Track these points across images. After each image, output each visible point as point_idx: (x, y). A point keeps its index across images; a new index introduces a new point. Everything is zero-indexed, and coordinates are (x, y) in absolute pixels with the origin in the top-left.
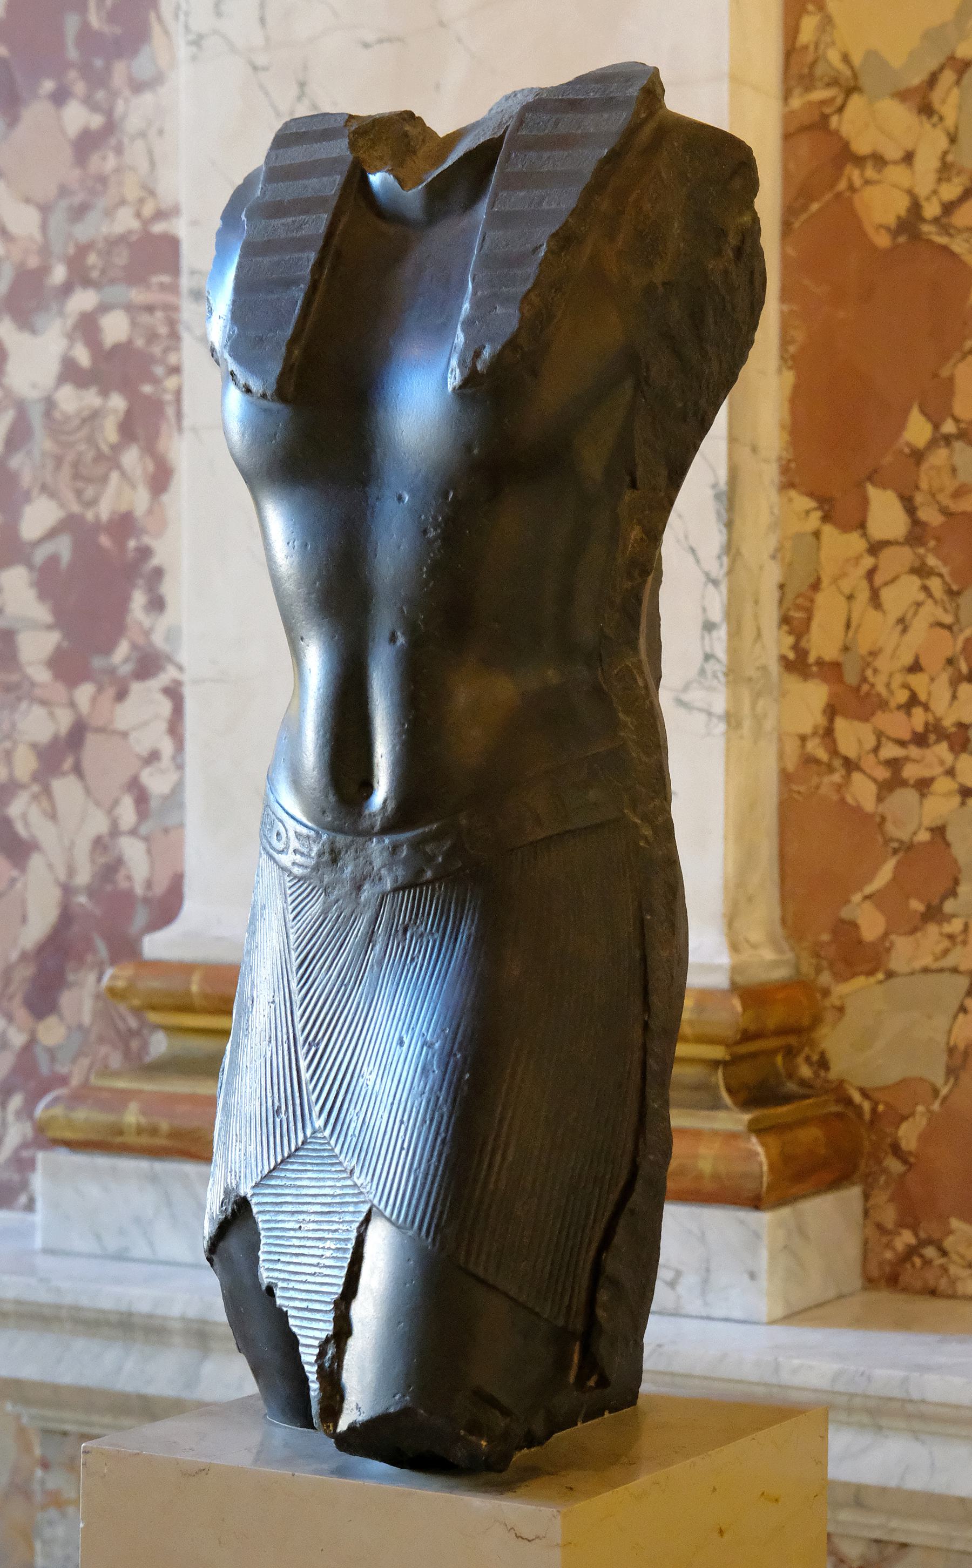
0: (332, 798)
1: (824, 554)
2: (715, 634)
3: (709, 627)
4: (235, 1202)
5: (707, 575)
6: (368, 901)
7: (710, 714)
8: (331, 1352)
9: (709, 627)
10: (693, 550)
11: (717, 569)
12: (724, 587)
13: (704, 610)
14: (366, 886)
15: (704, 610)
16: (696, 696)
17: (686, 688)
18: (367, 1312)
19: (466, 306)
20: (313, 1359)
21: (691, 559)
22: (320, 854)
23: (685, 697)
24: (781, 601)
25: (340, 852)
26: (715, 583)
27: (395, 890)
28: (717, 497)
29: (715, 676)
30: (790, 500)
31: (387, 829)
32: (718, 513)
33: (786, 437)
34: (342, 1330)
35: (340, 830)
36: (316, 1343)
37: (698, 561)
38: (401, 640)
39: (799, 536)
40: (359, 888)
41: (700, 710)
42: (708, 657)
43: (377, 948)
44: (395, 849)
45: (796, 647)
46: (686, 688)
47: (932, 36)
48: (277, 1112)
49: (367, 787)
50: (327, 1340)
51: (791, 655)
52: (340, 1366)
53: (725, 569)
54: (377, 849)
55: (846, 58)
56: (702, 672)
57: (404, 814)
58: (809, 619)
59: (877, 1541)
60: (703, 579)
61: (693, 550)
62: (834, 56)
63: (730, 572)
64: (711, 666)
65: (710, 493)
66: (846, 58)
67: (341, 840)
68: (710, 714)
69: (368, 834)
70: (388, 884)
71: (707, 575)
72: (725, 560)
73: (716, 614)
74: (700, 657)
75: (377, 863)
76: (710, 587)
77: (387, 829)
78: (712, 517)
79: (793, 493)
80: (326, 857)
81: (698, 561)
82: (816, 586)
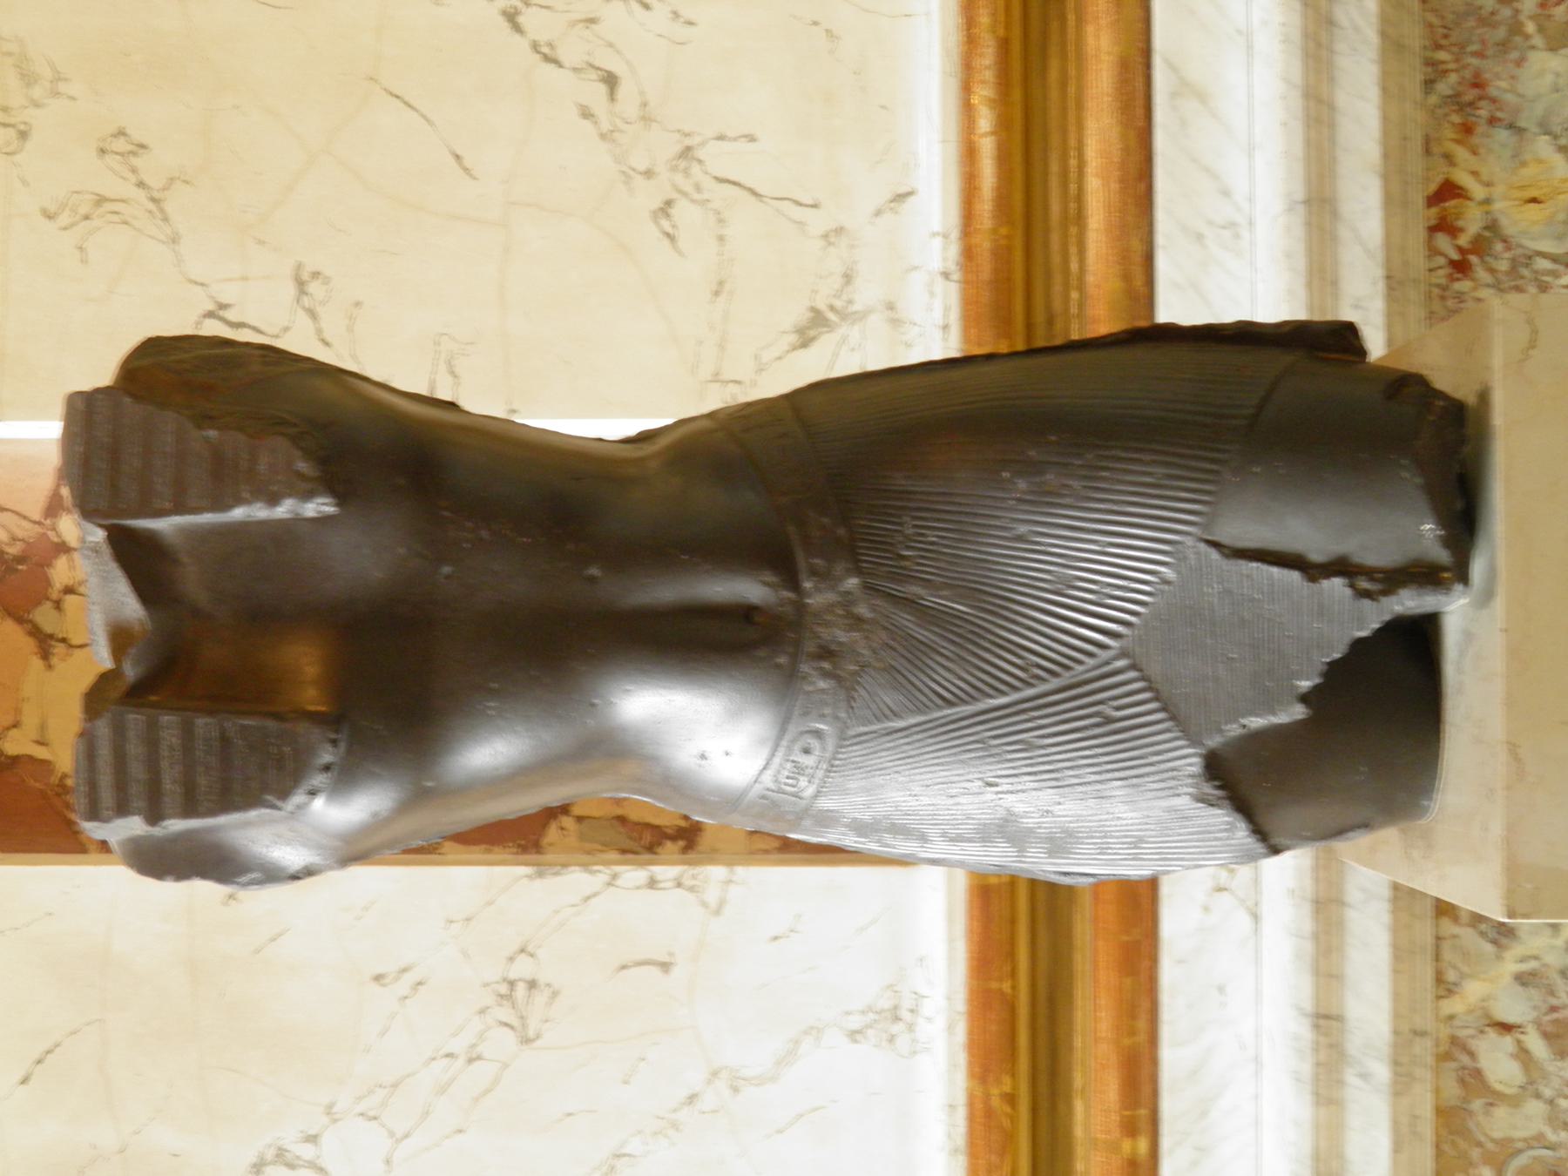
0: (761, 653)
1: (595, 813)
2: (659, 878)
5: (610, 884)
6: (873, 609)
8: (1364, 584)
9: (652, 883)
16: (712, 896)
17: (704, 904)
18: (1316, 542)
21: (593, 900)
22: (826, 675)
24: (636, 853)
25: (821, 647)
26: (615, 876)
27: (859, 572)
28: (540, 875)
30: (551, 844)
31: (793, 582)
32: (556, 874)
33: (496, 849)
34: (1341, 567)
35: (797, 644)
37: (595, 895)
38: (594, 571)
39: (582, 837)
40: (859, 619)
42: (679, 885)
44: (814, 573)
45: (673, 838)
46: (704, 904)
48: (1109, 720)
49: (746, 613)
50: (1352, 586)
51: (681, 843)
56: (692, 889)
57: (775, 557)
58: (648, 826)
60: (612, 889)
64: (688, 882)
65: (538, 883)
67: (810, 647)
69: (800, 608)
76: (619, 882)
77: (793, 582)
78: (558, 879)
79: (545, 841)
81: (595, 895)
82: (622, 820)
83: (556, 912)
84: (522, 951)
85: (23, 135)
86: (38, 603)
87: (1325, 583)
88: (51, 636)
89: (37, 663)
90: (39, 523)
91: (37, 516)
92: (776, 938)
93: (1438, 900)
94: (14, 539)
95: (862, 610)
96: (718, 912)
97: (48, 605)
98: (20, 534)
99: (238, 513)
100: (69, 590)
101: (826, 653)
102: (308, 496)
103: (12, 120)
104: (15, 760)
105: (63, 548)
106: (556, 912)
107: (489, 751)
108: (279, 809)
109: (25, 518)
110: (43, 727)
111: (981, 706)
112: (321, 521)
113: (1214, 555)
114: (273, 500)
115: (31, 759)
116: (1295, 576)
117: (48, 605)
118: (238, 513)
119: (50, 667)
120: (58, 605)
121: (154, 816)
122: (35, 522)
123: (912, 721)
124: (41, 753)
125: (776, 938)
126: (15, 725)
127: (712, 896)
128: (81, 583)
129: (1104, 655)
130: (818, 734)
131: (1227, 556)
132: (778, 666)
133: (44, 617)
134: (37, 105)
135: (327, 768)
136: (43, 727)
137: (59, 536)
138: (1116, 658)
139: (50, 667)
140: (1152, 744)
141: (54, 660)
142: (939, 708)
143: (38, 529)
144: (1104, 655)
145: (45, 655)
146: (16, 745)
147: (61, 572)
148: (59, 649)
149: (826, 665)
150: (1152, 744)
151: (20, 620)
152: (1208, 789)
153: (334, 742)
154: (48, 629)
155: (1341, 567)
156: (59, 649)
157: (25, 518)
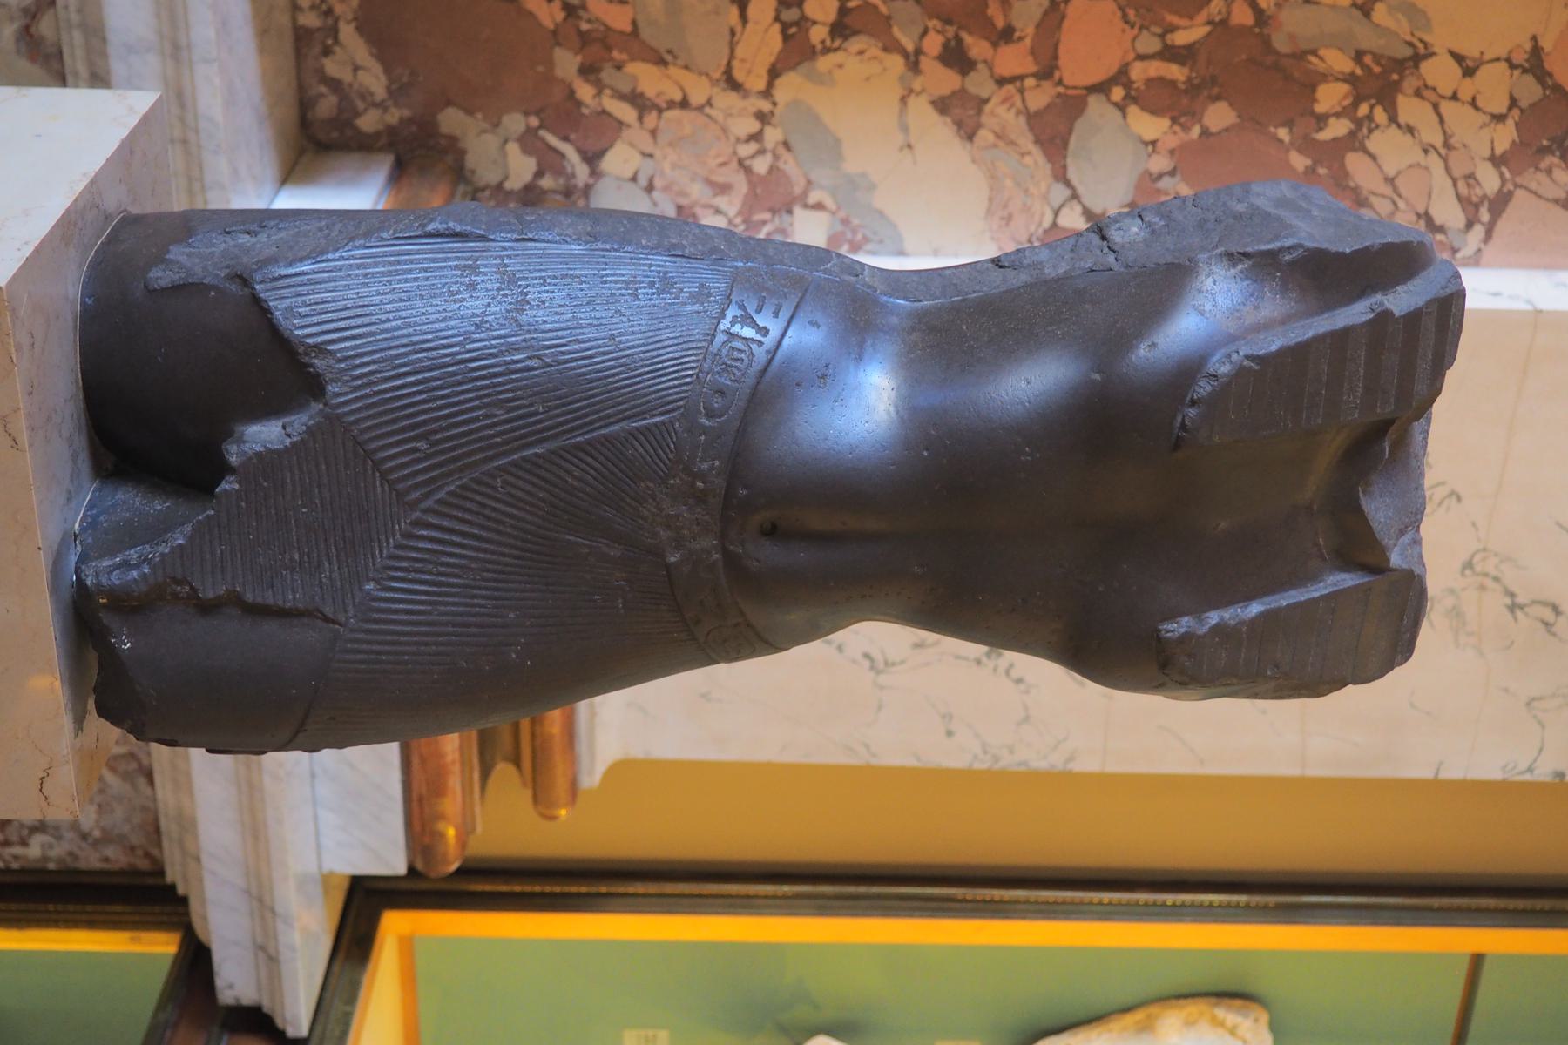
4: (317, 376)
14: (669, 533)
22: (702, 476)
27: (667, 566)
40: (668, 527)
54: (708, 542)
85: (1469, 565)
86: (1533, 106)
87: (221, 590)
88: (1525, 71)
89: (1547, 44)
90: (1516, 186)
91: (1519, 193)
93: (62, 80)
94: (1549, 171)
95: (664, 534)
97: (1524, 104)
98: (1542, 177)
99: (1255, 609)
100: (1499, 118)
101: (701, 498)
102: (1186, 638)
103: (1480, 579)
105: (1496, 161)
107: (1032, 382)
108: (1247, 357)
109: (1531, 192)
111: (552, 445)
112: (1174, 615)
113: (328, 610)
114: (1218, 629)
116: (249, 597)
117: (1524, 104)
118: (1255, 609)
119: (1534, 38)
120: (1513, 103)
121: (1384, 316)
122: (1521, 186)
123: (616, 427)
128: (1485, 125)
129: (429, 503)
130: (710, 414)
131: (318, 610)
132: (745, 487)
133: (1530, 90)
134: (1452, 591)
135: (1193, 403)
137: (1502, 175)
138: (419, 501)
139: (1534, 38)
140: (380, 414)
141: (1528, 46)
142: (588, 442)
143: (1518, 180)
144: (429, 503)
145: (1536, 51)
147: (1505, 136)
148: (1519, 58)
149: (700, 485)
150: (380, 414)
151: (1557, 88)
152: (319, 363)
153: (1183, 426)
154: (1529, 78)
155: (208, 608)
156: (1519, 58)
157: (1531, 192)
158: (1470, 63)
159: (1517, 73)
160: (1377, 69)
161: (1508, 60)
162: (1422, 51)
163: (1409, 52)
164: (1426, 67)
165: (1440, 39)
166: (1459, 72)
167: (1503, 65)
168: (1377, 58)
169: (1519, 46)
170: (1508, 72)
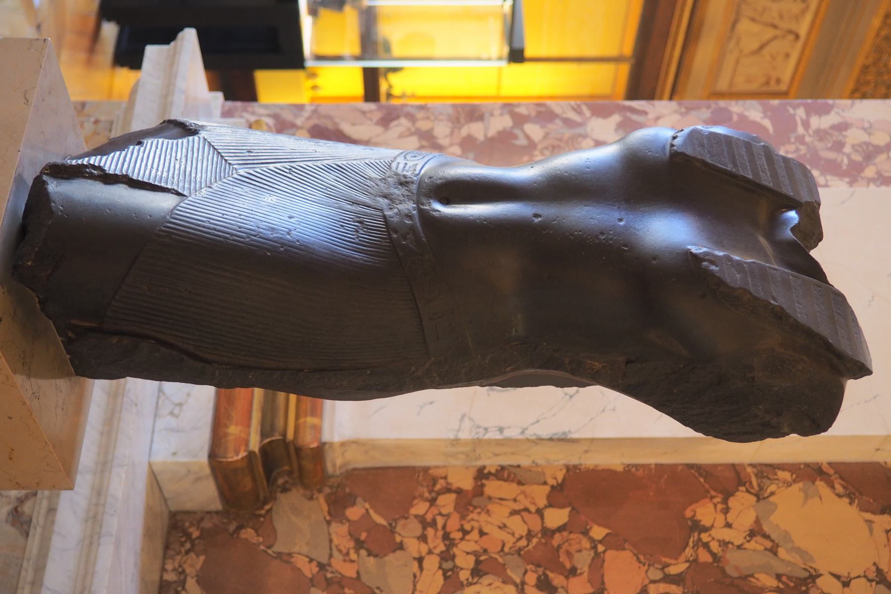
0: (439, 182)
1: (535, 487)
2: (498, 433)
3: (501, 430)
5: (526, 429)
7: (458, 431)
9: (501, 430)
10: (538, 421)
11: (529, 434)
12: (521, 437)
13: (509, 427)
15: (509, 427)
16: (467, 423)
17: (471, 419)
18: (121, 195)
19: (738, 258)
20: (92, 162)
22: (405, 176)
23: (466, 419)
24: (511, 466)
26: (523, 433)
27: (384, 217)
28: (564, 433)
29: (477, 433)
30: (561, 470)
32: (556, 434)
33: (591, 467)
36: (102, 164)
37: (533, 424)
38: (537, 220)
39: (543, 474)
40: (385, 196)
41: (460, 426)
42: (486, 429)
43: (349, 207)
44: (409, 216)
45: (490, 473)
46: (471, 419)
47: (787, 536)
49: (446, 202)
50: (103, 170)
51: (486, 471)
52: (86, 178)
53: (529, 437)
55: (772, 494)
56: (479, 427)
58: (505, 480)
59: (31, 520)
61: (538, 421)
62: (773, 488)
63: (528, 440)
64: (481, 431)
65: (566, 430)
66: (772, 494)
67: (414, 187)
68: (458, 431)
69: (418, 203)
70: (387, 213)
71: (526, 429)
72: (534, 437)
73: (508, 434)
74: (486, 425)
75: (401, 207)
76: (521, 430)
79: (564, 471)
80: (403, 180)
81: (533, 424)
82: (520, 483)
83: (554, 415)
84: (571, 397)
88: (877, 583)
89: (884, 567)
92: (431, 403)
96: (464, 416)
104: (883, 512)
106: (554, 415)
110: (871, 531)
115: (873, 513)
119: (875, 564)
124: (869, 516)
125: (431, 403)
126: (887, 532)
127: (467, 423)
136: (871, 531)
141: (874, 568)
145: (879, 571)
146: (884, 521)
148: (872, 575)
156: (872, 575)
158: (845, 580)
159: (874, 584)
160: (792, 584)
161: (865, 576)
162: (814, 574)
163: (806, 574)
164: (819, 581)
165: (822, 566)
166: (840, 585)
167: (863, 580)
168: (790, 578)
169: (868, 569)
170: (868, 584)
